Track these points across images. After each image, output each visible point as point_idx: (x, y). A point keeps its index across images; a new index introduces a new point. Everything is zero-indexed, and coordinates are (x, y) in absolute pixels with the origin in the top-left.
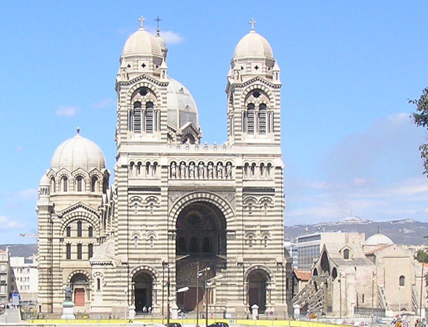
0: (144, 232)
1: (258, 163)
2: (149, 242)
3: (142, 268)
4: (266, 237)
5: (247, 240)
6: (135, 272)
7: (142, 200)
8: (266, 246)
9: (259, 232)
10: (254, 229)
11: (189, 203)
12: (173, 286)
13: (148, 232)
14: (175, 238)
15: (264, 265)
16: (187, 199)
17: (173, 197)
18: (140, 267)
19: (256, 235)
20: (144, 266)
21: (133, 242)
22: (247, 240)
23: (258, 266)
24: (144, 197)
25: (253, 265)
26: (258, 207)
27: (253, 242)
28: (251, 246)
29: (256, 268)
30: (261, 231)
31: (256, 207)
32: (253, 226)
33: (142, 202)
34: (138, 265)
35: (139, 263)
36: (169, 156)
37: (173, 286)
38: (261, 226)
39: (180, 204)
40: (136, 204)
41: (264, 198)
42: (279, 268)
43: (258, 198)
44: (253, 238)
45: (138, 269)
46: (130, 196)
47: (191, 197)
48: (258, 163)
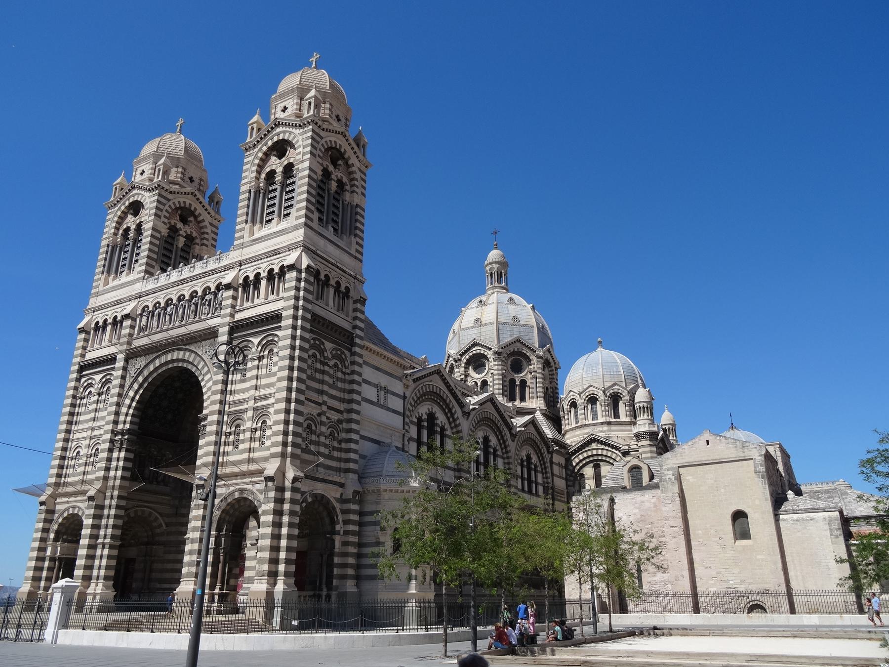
0: (87, 441)
1: (264, 271)
2: (92, 459)
3: (71, 512)
4: (264, 422)
5: (230, 433)
6: (60, 520)
7: (96, 383)
8: (263, 443)
9: (250, 413)
10: (245, 406)
11: (155, 375)
12: (103, 548)
13: (94, 440)
14: (125, 446)
15: (250, 487)
16: (151, 368)
17: (133, 369)
18: (67, 509)
19: (246, 419)
20: (74, 507)
21: (73, 462)
22: (230, 433)
23: (241, 491)
24: (98, 377)
25: (232, 488)
26: (254, 360)
27: (241, 437)
28: (237, 447)
29: (237, 495)
30: (255, 409)
31: (253, 360)
32: (242, 402)
33: (96, 386)
34: (66, 506)
35: (68, 502)
36: (141, 299)
37: (103, 548)
38: (256, 400)
39: (141, 379)
40: (90, 392)
41: (265, 337)
42: (267, 490)
43: (256, 340)
44: (242, 428)
45: (65, 515)
46: (83, 380)
47: (157, 363)
48: (264, 271)
